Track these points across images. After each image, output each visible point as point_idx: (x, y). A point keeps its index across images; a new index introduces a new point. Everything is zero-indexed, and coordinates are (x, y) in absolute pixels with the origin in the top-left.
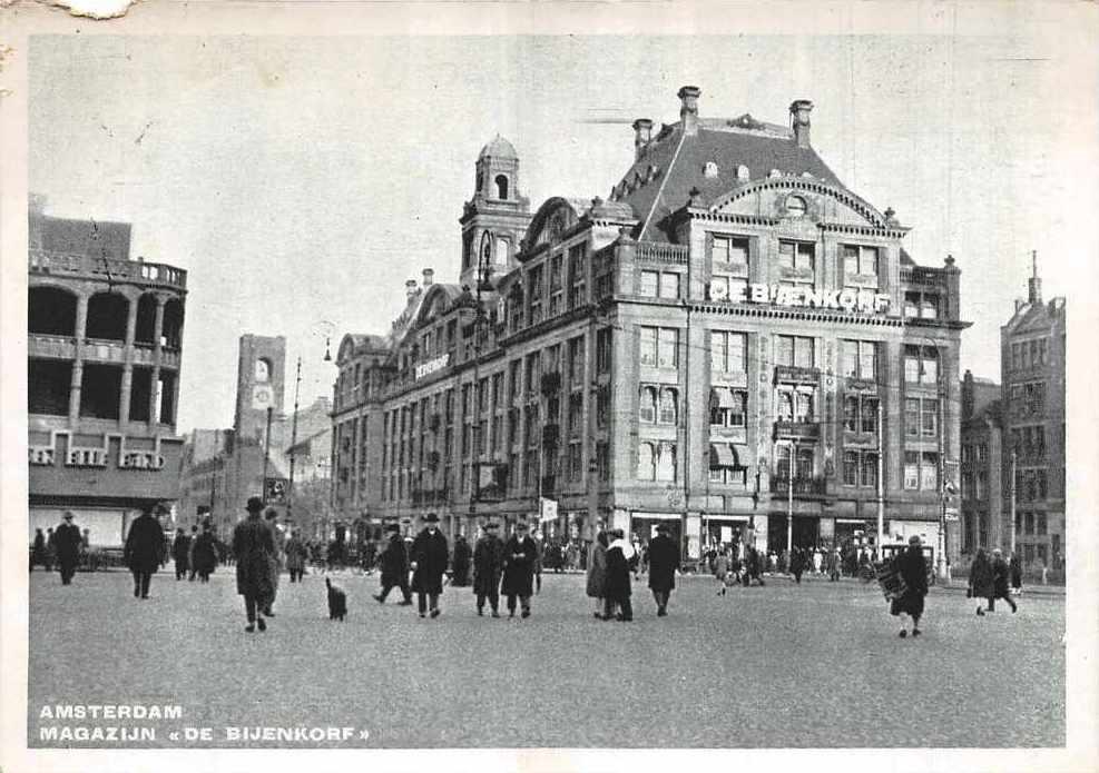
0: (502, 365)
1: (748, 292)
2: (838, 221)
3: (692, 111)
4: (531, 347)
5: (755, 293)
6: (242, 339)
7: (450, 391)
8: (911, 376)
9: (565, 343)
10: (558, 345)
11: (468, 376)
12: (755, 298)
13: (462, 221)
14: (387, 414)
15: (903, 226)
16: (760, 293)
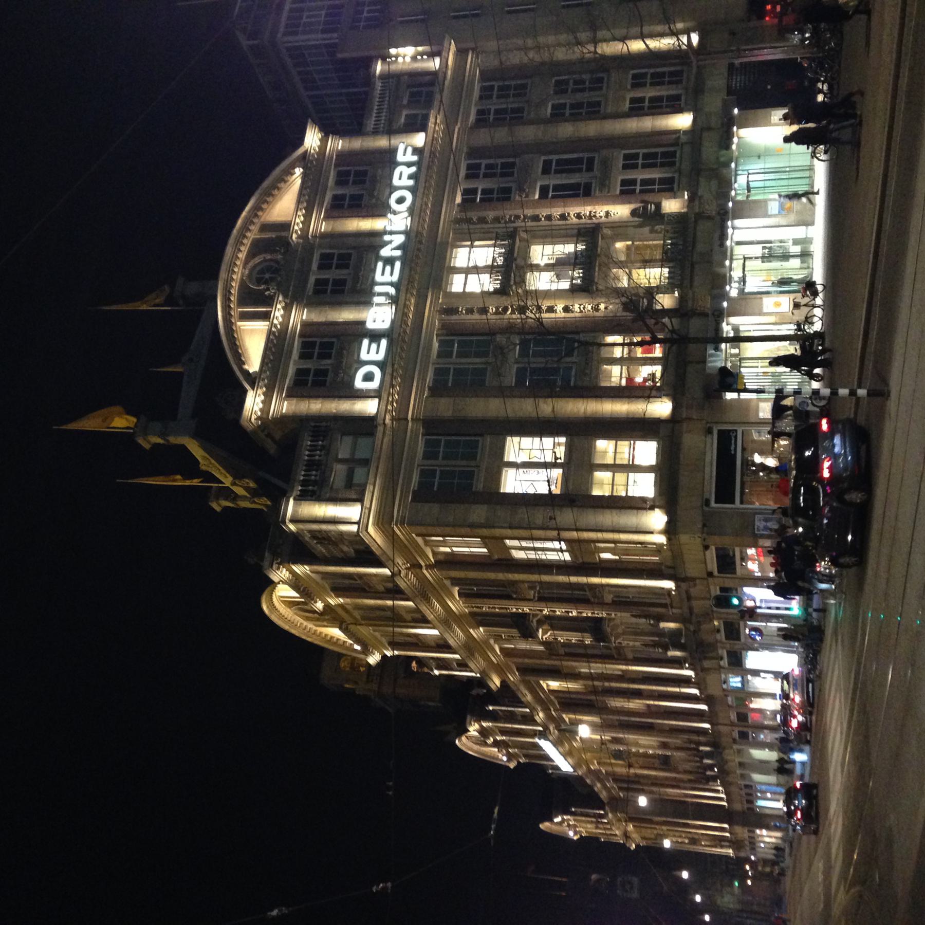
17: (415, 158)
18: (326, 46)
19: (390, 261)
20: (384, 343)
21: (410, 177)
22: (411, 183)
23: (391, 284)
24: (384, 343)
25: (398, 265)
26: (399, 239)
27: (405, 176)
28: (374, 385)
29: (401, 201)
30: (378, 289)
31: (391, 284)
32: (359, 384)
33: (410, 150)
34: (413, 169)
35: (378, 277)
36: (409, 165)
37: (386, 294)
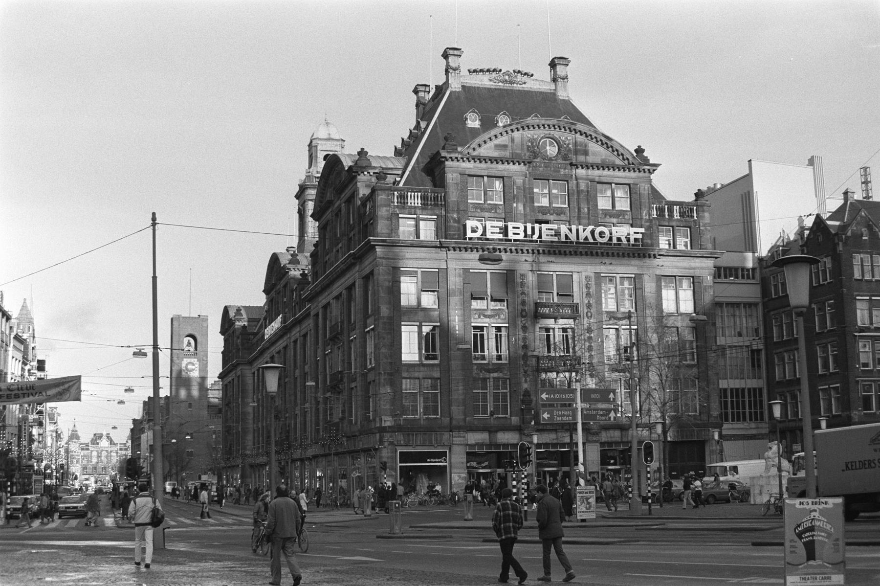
0: (309, 323)
1: (505, 231)
2: (590, 159)
3: (455, 69)
4: (323, 300)
5: (511, 231)
6: (172, 319)
7: (285, 348)
8: (668, 305)
9: (344, 292)
10: (340, 294)
11: (295, 333)
12: (511, 236)
13: (298, 197)
14: (254, 373)
15: (651, 162)
16: (516, 231)
17: (632, 241)
19: (557, 234)
20: (501, 236)
22: (615, 241)
23: (540, 236)
24: (501, 236)
25: (556, 239)
26: (573, 237)
28: (469, 234)
29: (602, 234)
31: (540, 236)
33: (640, 236)
34: (624, 241)
37: (533, 233)
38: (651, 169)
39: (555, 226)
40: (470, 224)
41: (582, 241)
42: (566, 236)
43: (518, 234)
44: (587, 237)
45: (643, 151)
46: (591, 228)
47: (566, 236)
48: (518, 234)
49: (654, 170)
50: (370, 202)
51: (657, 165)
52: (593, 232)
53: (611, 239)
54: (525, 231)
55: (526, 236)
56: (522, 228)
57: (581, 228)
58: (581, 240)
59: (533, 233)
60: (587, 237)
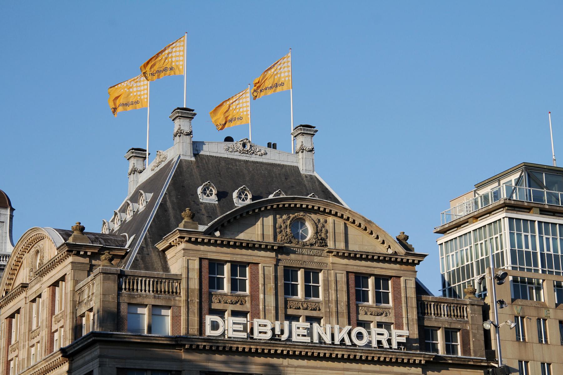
12: (256, 335)
15: (416, 251)
16: (263, 329)
17: (395, 346)
18: (502, 252)
21: (379, 342)
22: (374, 344)
24: (244, 335)
25: (308, 339)
26: (328, 340)
27: (380, 338)
28: (208, 332)
29: (360, 336)
30: (286, 323)
32: (209, 319)
34: (385, 345)
35: (294, 324)
36: (389, 341)
37: (282, 332)
38: (416, 259)
39: (308, 325)
40: (209, 319)
41: (339, 343)
42: (320, 337)
43: (265, 333)
44: (343, 340)
45: (407, 238)
46: (348, 328)
47: (320, 337)
48: (265, 333)
49: (419, 261)
50: (89, 287)
51: (425, 256)
52: (349, 334)
53: (370, 342)
54: (273, 330)
55: (274, 334)
56: (269, 327)
57: (337, 327)
58: (337, 342)
59: (282, 332)
60: (343, 340)
